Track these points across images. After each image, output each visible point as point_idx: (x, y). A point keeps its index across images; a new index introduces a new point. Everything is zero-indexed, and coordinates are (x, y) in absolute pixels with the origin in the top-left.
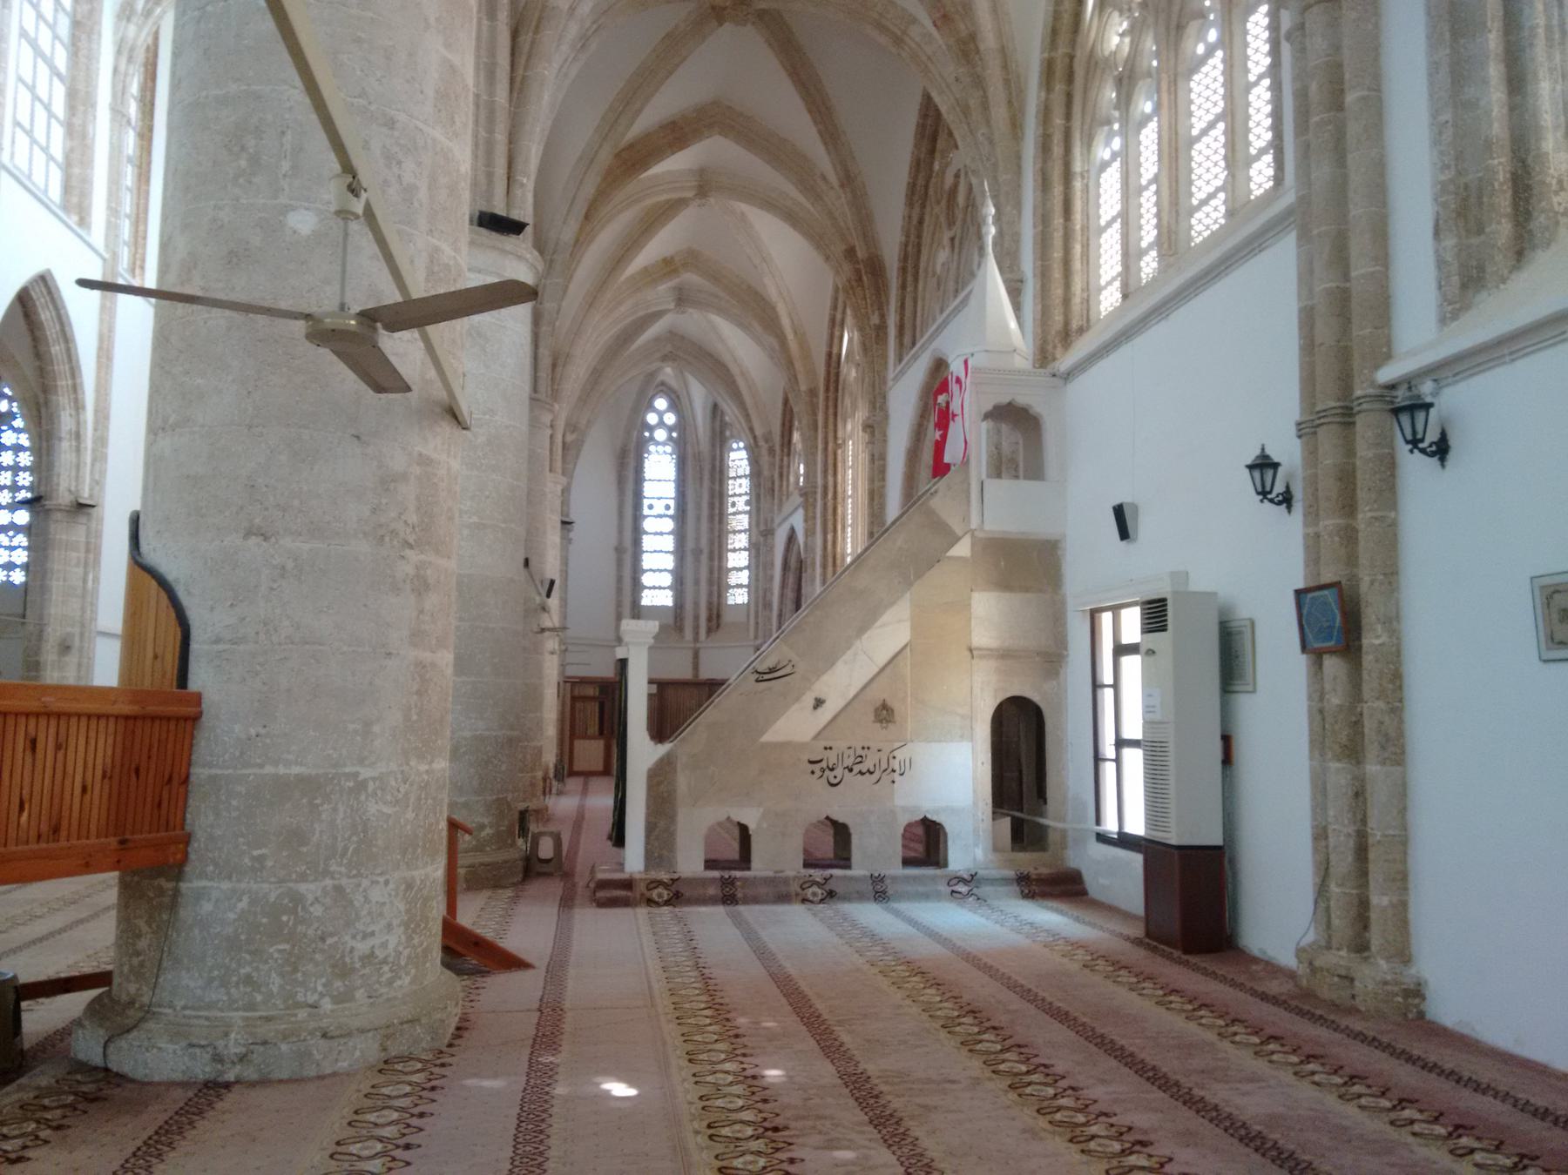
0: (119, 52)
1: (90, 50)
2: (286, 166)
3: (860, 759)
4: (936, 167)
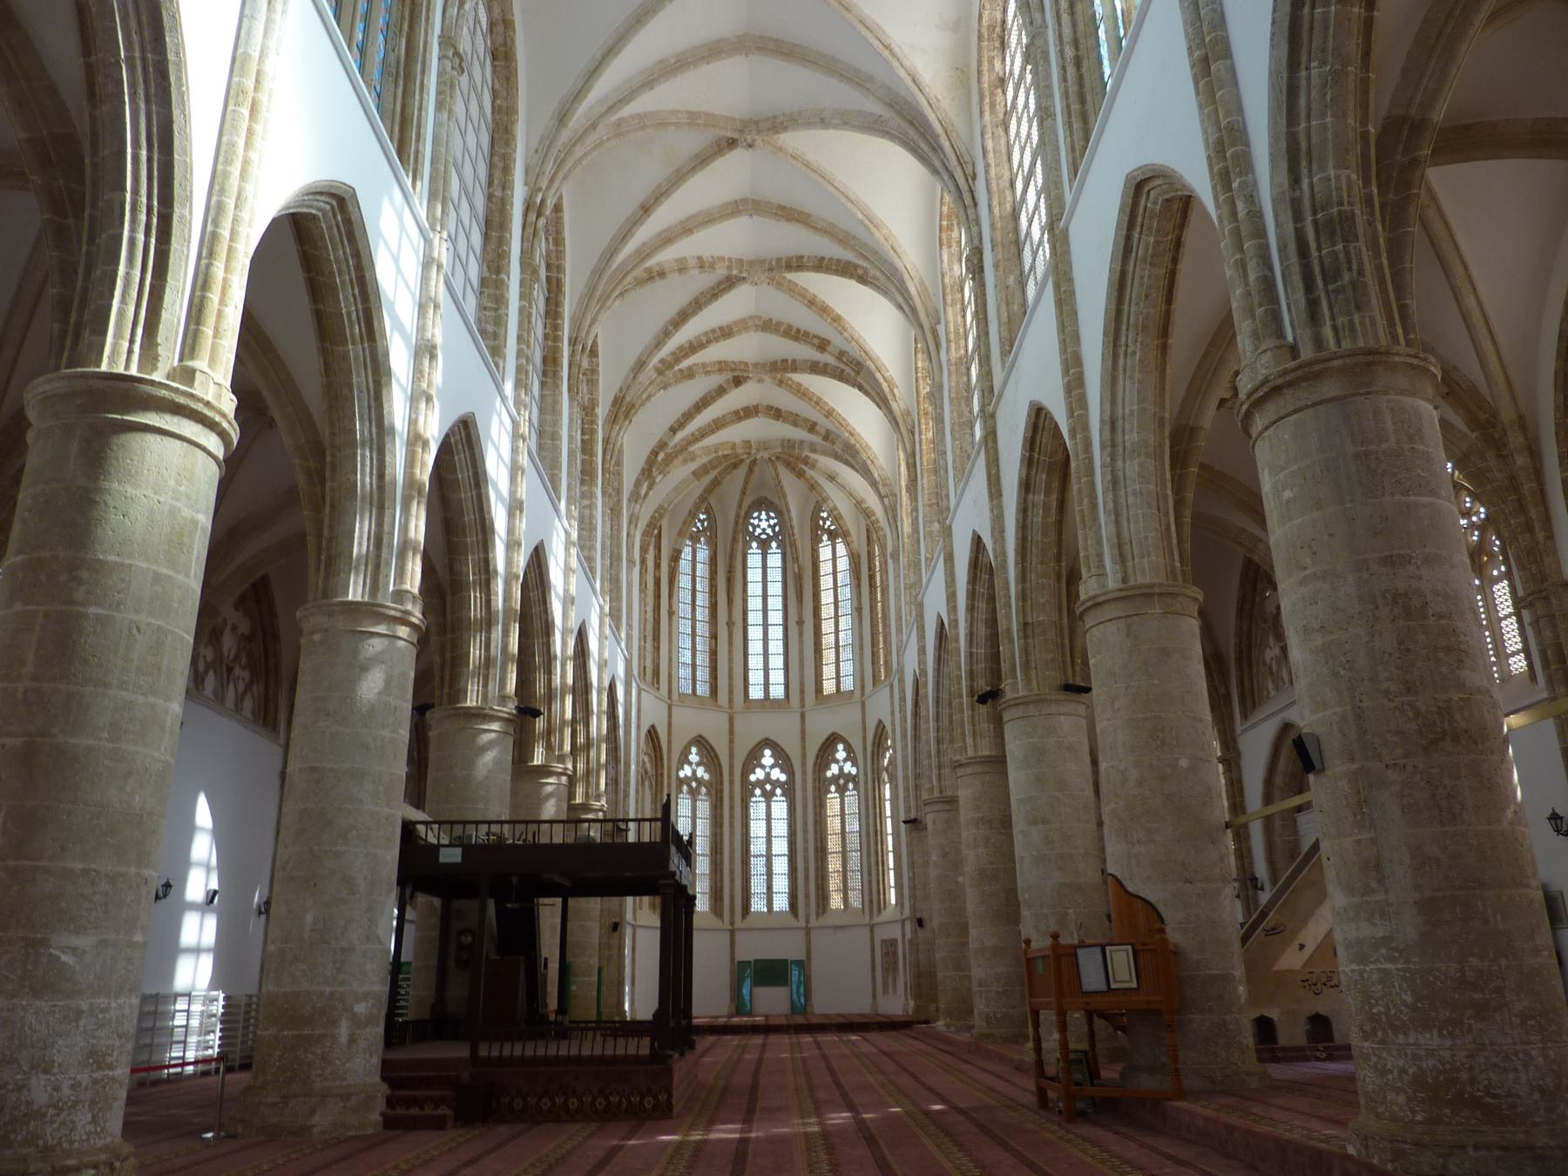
0: (630, 523)
1: (619, 525)
2: (1174, 743)
3: (1330, 979)
4: (1257, 599)
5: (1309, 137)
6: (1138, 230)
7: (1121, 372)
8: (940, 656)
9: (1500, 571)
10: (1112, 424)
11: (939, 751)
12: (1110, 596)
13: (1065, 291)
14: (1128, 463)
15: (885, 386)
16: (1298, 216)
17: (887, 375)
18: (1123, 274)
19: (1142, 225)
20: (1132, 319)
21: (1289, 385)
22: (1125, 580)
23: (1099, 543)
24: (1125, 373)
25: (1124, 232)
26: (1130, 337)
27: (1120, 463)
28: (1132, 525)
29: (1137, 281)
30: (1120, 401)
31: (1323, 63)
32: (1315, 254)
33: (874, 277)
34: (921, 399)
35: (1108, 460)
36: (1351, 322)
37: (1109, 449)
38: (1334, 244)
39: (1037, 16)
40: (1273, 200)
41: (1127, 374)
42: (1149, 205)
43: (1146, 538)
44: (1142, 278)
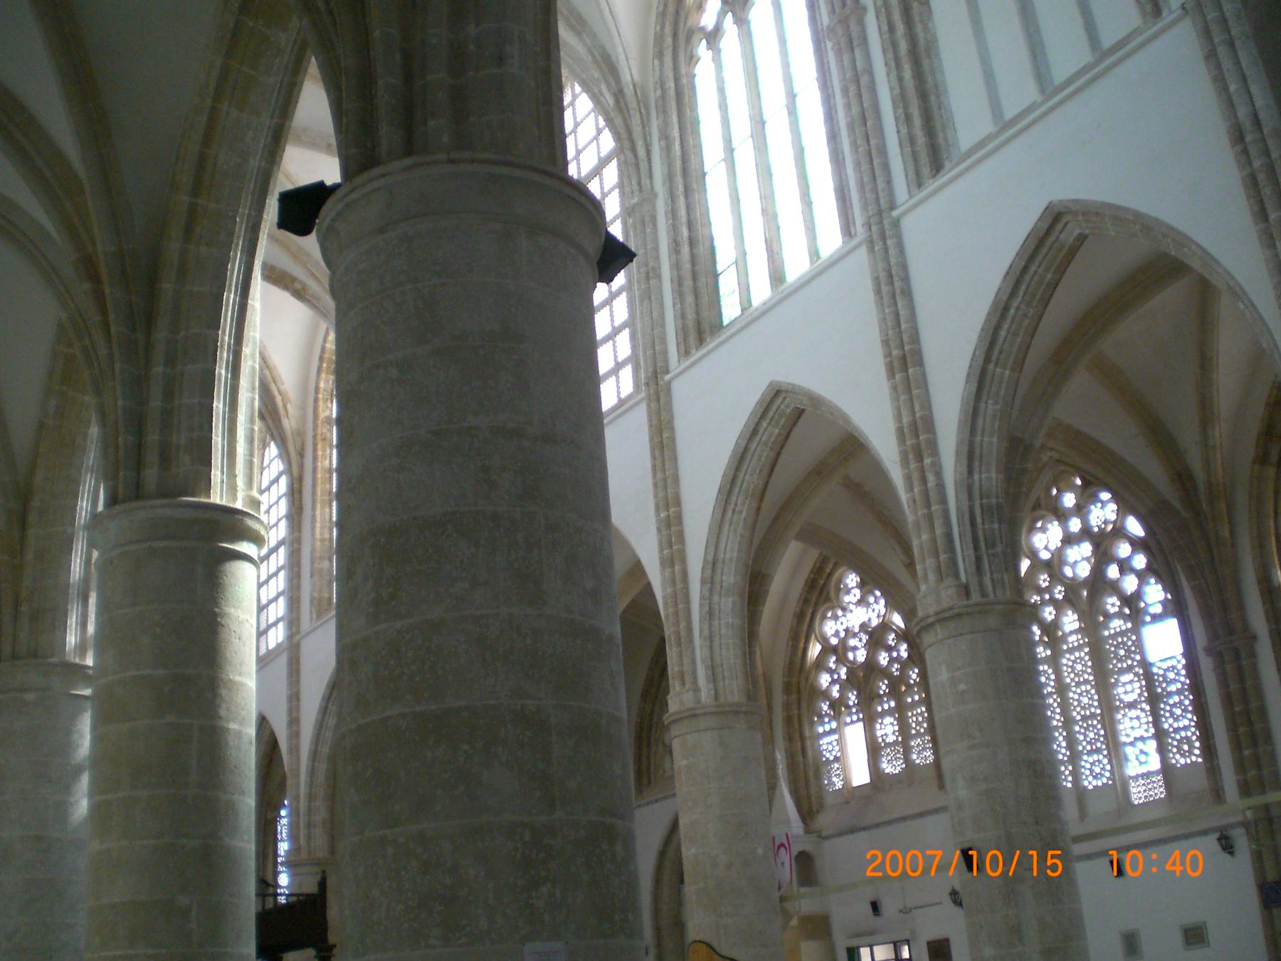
5: (981, 446)
6: (768, 421)
7: (727, 525)
8: (326, 708)
9: (913, 700)
10: (712, 565)
11: (309, 809)
12: (707, 710)
13: (668, 438)
14: (723, 600)
15: (279, 399)
16: (970, 497)
17: (282, 388)
18: (746, 450)
19: (772, 418)
20: (745, 485)
21: (968, 614)
22: (716, 697)
23: (694, 662)
24: (730, 525)
25: (756, 420)
26: (740, 498)
27: (716, 598)
28: (724, 651)
29: (755, 458)
30: (722, 546)
31: (996, 403)
32: (980, 526)
33: (313, 296)
34: (320, 422)
35: (707, 594)
36: (1002, 578)
37: (709, 585)
38: (992, 522)
39: (645, 181)
40: (956, 484)
41: (733, 526)
42: (782, 407)
43: (735, 664)
44: (760, 457)
